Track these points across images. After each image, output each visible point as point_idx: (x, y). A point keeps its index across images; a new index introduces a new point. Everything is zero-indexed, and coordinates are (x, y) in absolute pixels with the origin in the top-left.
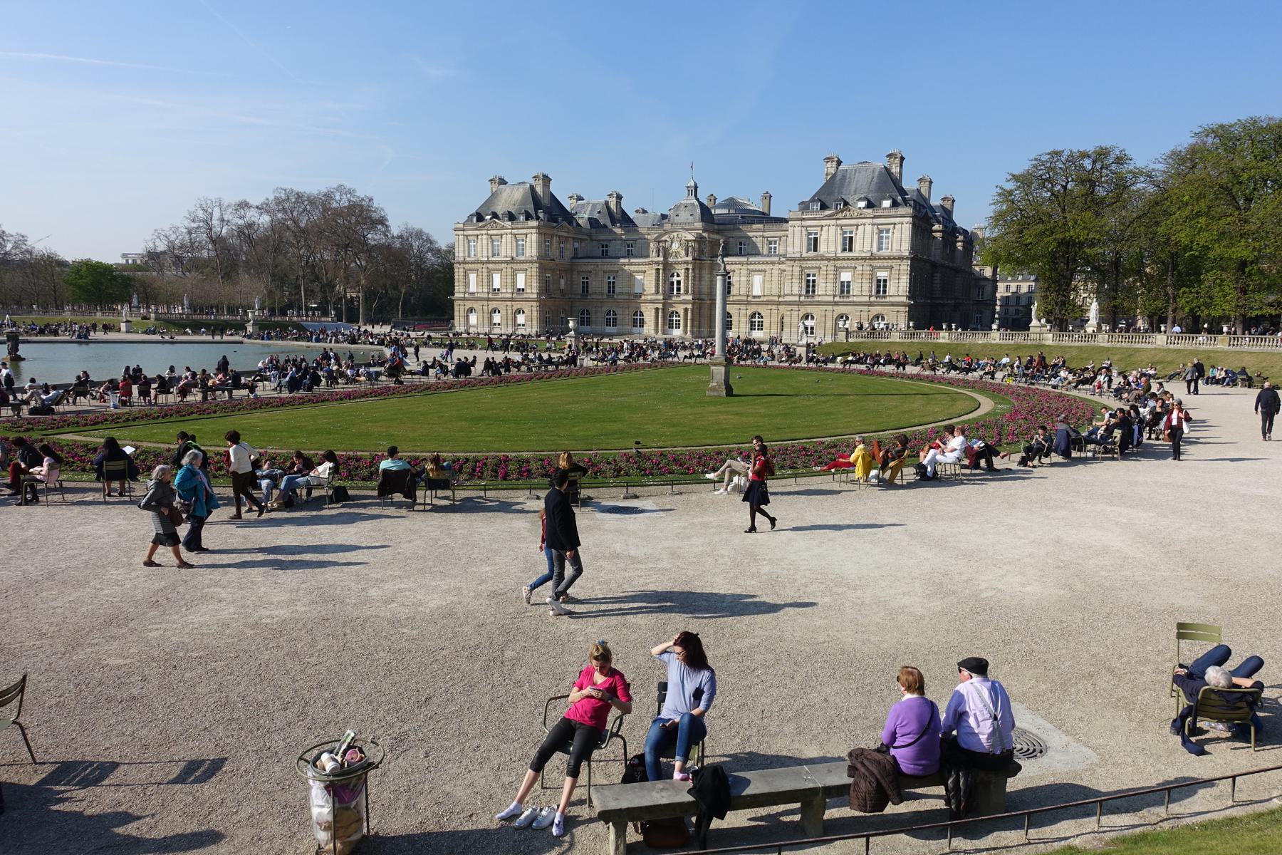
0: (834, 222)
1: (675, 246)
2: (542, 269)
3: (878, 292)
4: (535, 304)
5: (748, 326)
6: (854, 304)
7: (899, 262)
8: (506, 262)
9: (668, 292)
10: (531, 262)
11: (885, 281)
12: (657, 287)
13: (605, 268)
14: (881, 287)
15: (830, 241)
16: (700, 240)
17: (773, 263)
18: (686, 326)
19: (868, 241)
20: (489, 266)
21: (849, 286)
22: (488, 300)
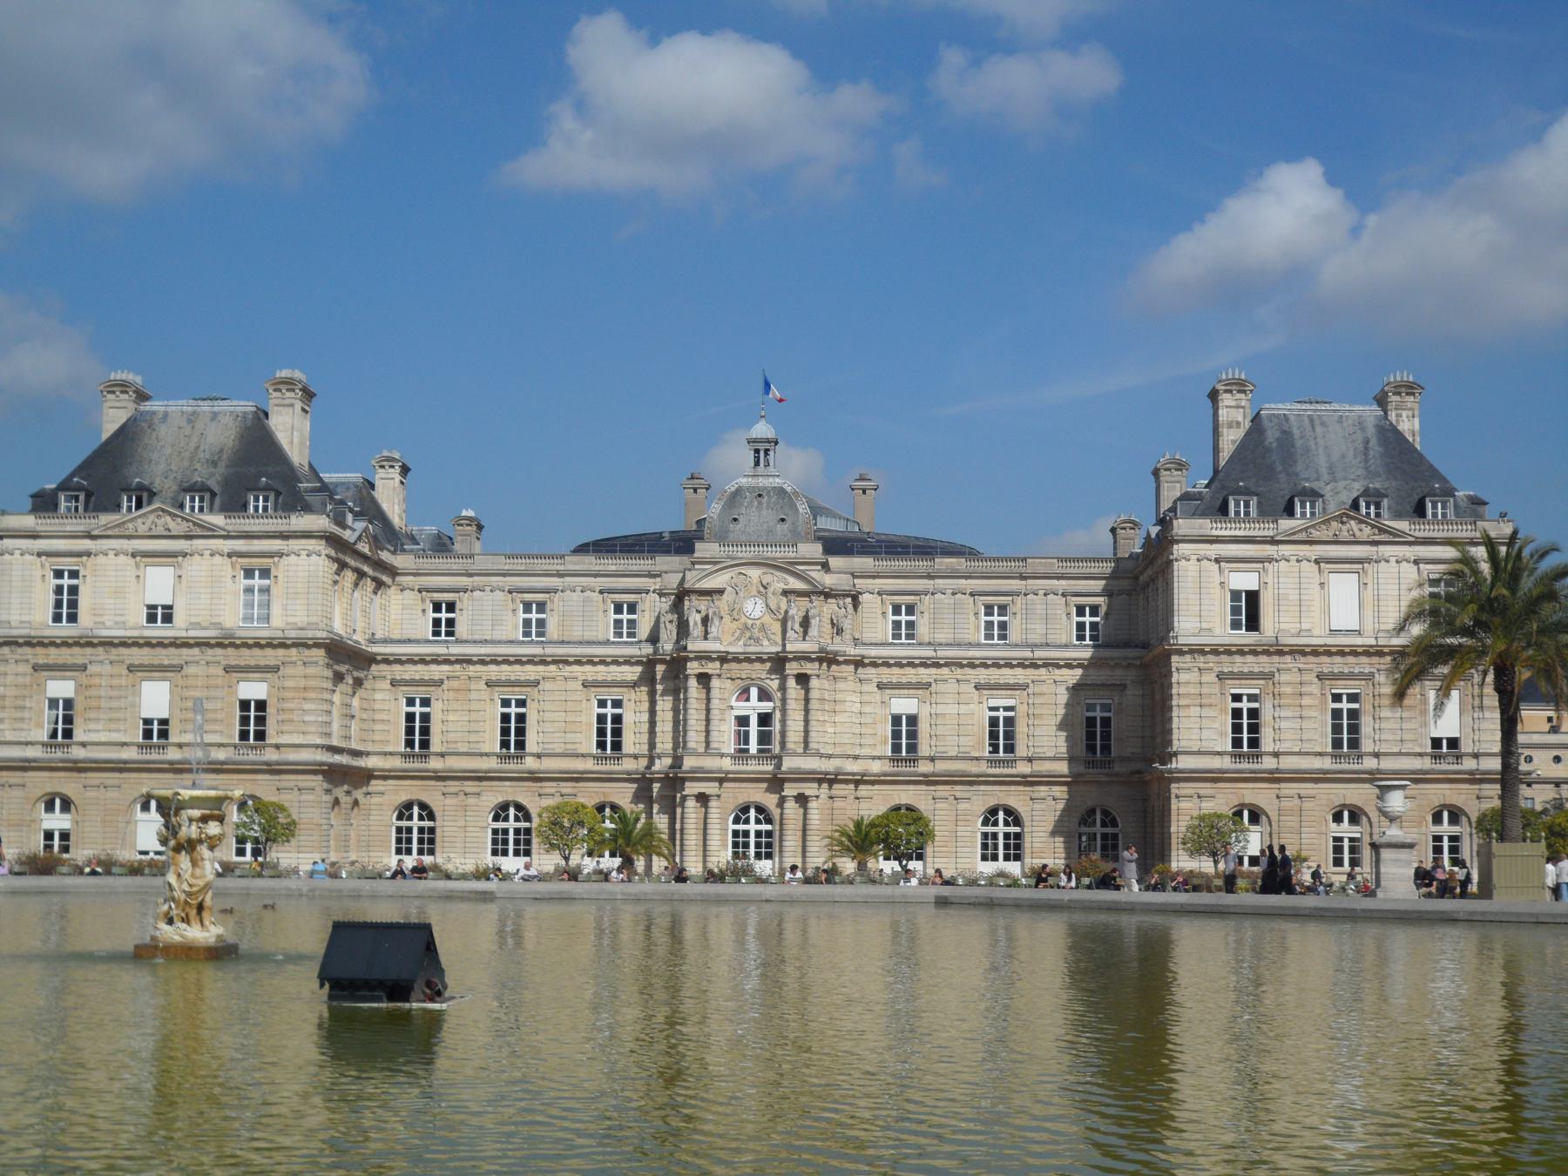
1: (754, 608)
9: (730, 748)
22: (121, 767)
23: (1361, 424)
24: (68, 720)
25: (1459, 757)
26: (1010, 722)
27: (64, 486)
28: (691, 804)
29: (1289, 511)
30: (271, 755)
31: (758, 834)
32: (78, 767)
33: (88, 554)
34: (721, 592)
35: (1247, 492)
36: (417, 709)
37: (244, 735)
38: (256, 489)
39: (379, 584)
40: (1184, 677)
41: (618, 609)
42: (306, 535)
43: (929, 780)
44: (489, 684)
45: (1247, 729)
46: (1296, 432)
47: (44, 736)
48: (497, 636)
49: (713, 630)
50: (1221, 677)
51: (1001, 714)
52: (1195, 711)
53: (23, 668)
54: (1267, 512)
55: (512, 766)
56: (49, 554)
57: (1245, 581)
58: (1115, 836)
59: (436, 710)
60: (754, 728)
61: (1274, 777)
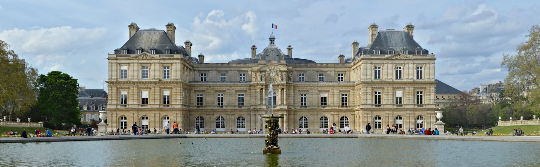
0: (390, 62)
2: (184, 89)
3: (418, 102)
4: (179, 112)
5: (319, 126)
6: (406, 110)
7: (429, 85)
8: (155, 83)
10: (177, 83)
11: (421, 96)
12: (262, 101)
13: (216, 88)
14: (419, 100)
15: (387, 72)
16: (288, 72)
17: (334, 86)
19: (411, 73)
20: (140, 85)
21: (400, 99)
22: (138, 110)
23: (401, 34)
24: (126, 100)
26: (325, 98)
27: (122, 48)
29: (387, 54)
30: (170, 107)
32: (128, 110)
33: (129, 63)
34: (265, 71)
35: (379, 49)
36: (200, 97)
37: (165, 103)
38: (166, 49)
39: (191, 70)
41: (241, 75)
42: (177, 59)
43: (310, 110)
44: (216, 91)
47: (119, 103)
48: (215, 81)
50: (373, 89)
54: (383, 53)
55: (220, 109)
56: (120, 63)
58: (348, 122)
59: (204, 97)
61: (385, 110)
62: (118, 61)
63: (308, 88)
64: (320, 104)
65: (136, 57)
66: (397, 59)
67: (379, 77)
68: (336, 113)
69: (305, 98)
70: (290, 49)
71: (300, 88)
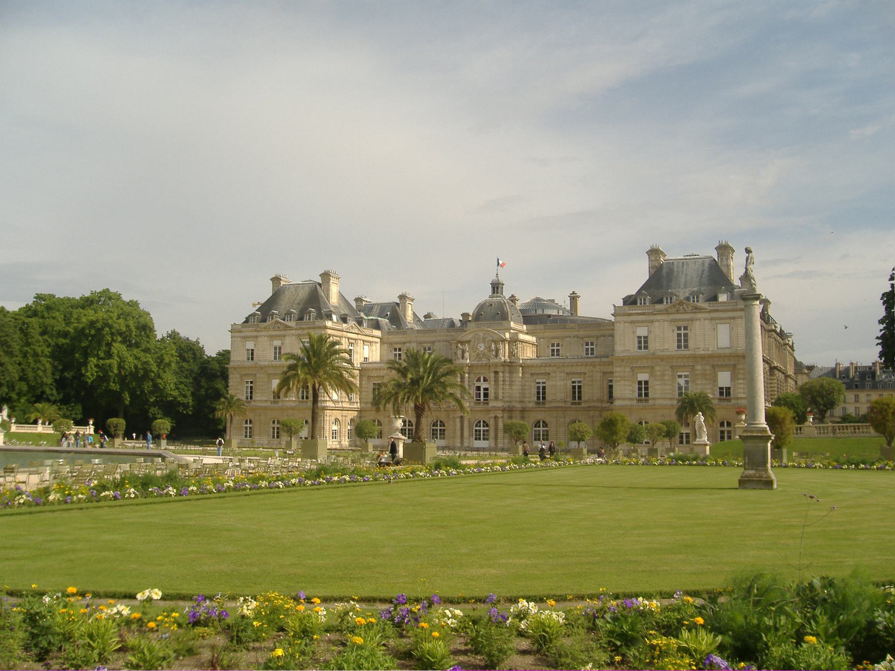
0: (665, 317)
18: (496, 438)
22: (265, 408)
25: (729, 400)
28: (458, 420)
29: (660, 301)
31: (484, 431)
33: (256, 337)
40: (618, 369)
45: (644, 388)
46: (675, 269)
49: (467, 355)
51: (577, 384)
52: (623, 382)
53: (237, 376)
56: (244, 337)
57: (642, 331)
60: (482, 392)
62: (242, 334)
63: (548, 370)
64: (570, 399)
65: (265, 328)
66: (678, 312)
67: (646, 348)
68: (597, 413)
69: (544, 388)
70: (574, 298)
71: (534, 371)
